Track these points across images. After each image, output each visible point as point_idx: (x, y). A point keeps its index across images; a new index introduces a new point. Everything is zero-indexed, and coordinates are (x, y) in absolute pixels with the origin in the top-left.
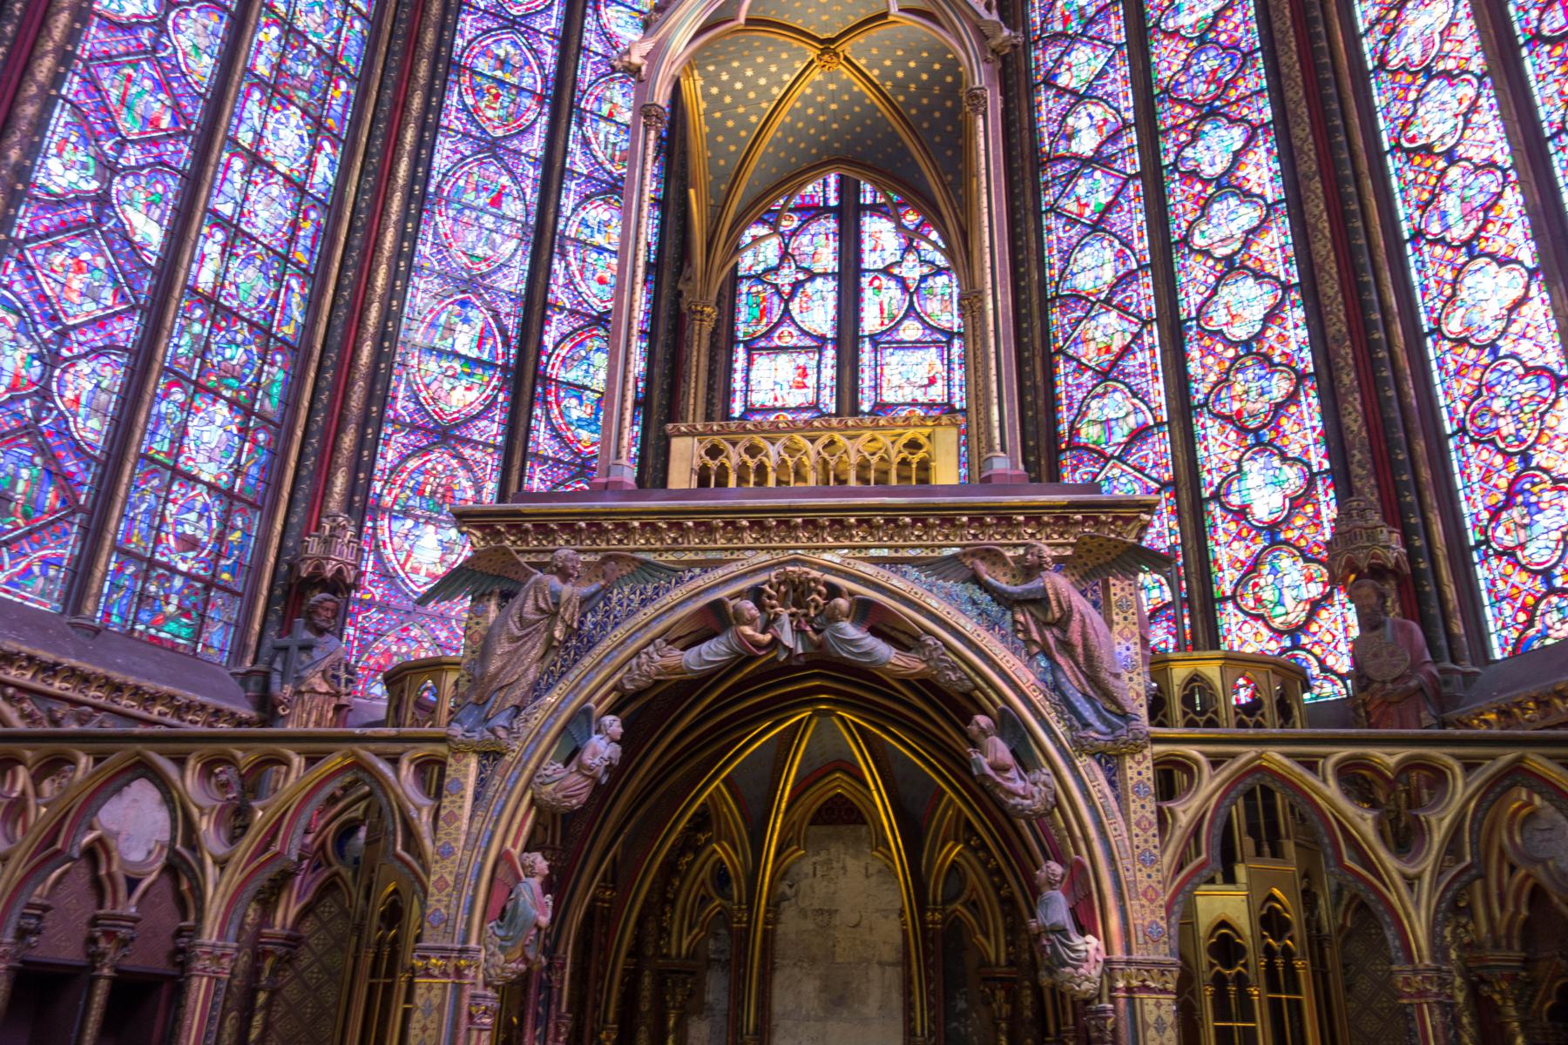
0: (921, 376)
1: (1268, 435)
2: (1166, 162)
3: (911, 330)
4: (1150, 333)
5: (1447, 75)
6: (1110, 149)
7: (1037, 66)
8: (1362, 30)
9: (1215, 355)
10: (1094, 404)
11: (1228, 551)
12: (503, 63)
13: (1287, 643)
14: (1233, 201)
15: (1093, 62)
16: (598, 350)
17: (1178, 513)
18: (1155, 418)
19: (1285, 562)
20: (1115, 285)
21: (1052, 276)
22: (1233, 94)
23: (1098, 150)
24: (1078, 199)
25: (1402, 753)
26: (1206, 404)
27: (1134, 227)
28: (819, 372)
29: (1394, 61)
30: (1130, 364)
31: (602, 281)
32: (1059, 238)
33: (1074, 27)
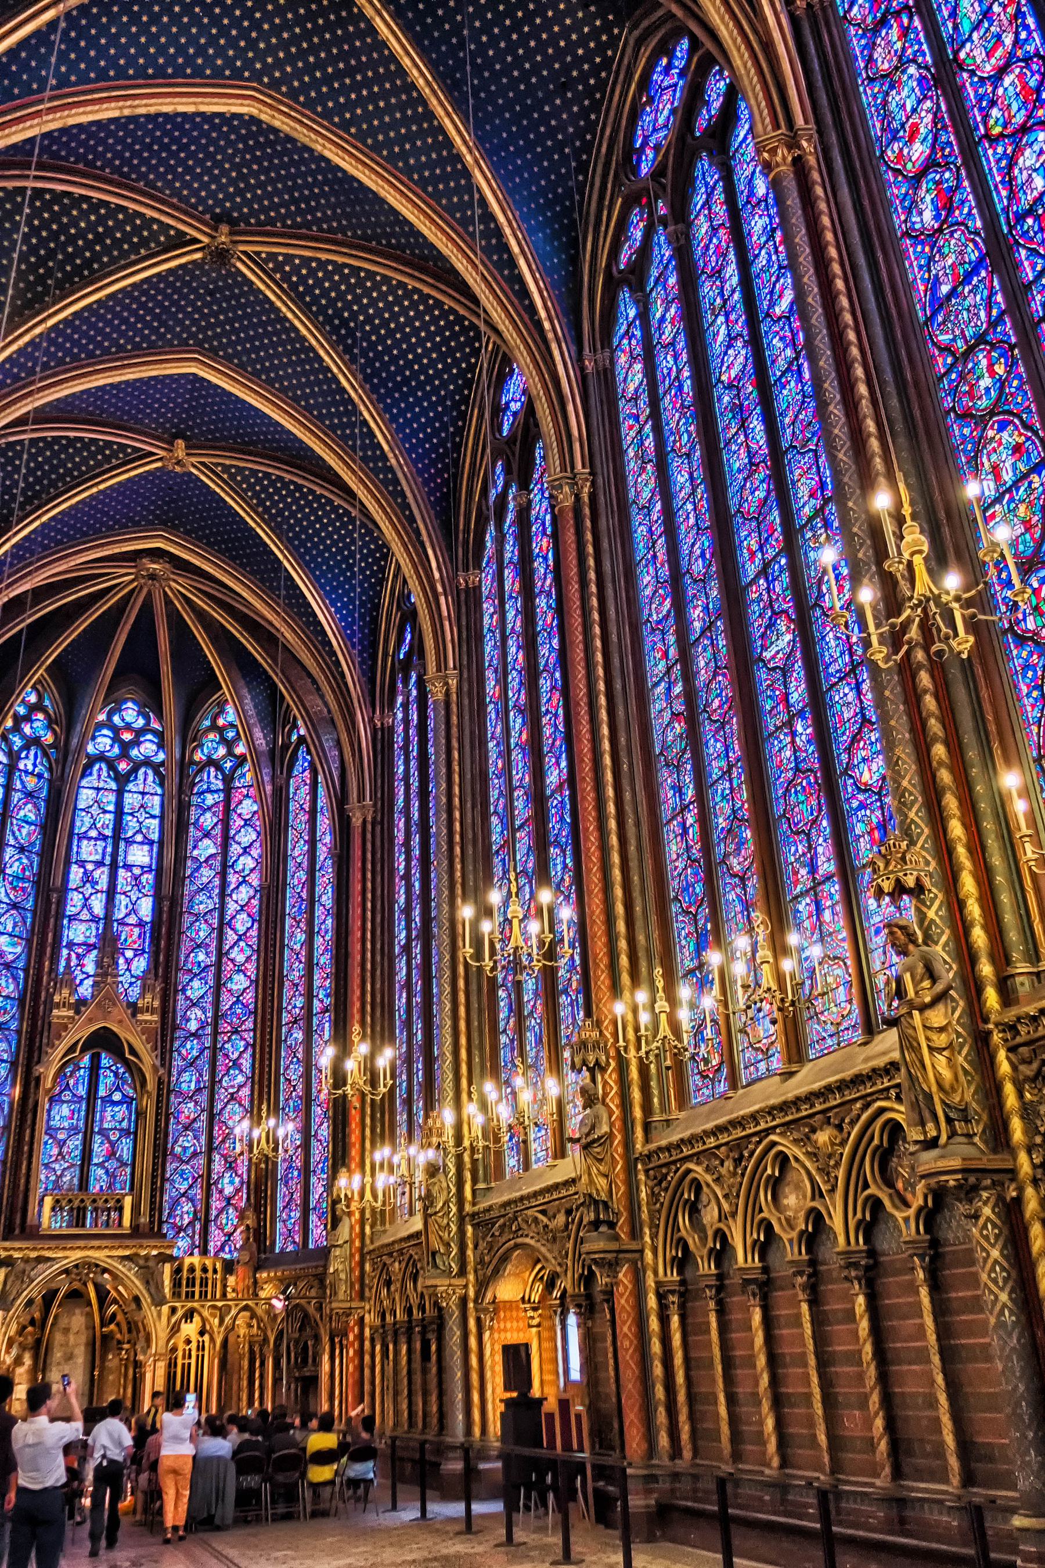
11: (216, 1204)
30: (196, 1125)
33: (196, 970)
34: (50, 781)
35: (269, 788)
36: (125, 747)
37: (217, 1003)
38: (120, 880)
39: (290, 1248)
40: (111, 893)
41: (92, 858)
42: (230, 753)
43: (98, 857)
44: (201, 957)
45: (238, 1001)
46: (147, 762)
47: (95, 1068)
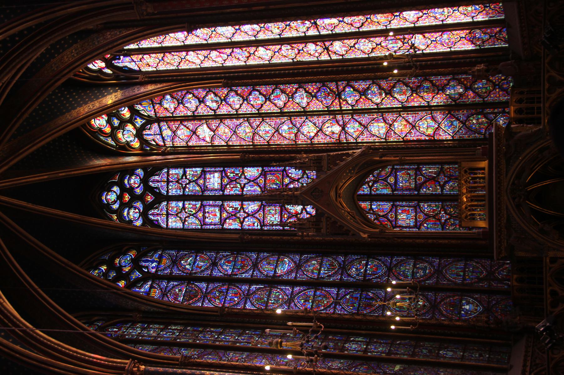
0: (406, 177)
1: (440, 88)
3: (392, 180)
5: (355, 44)
6: (341, 123)
7: (305, 142)
8: (329, 58)
9: (414, 99)
10: (421, 130)
12: (306, 301)
14: (370, 92)
16: (400, 269)
17: (458, 111)
19: (476, 86)
20: (386, 123)
23: (340, 126)
24: (355, 132)
25: (546, 83)
28: (404, 206)
29: (344, 53)
30: (411, 120)
31: (377, 269)
33: (295, 131)
34: (164, 250)
35: (150, 88)
36: (135, 198)
37: (318, 113)
38: (232, 192)
39: (504, 34)
40: (241, 198)
41: (218, 215)
42: (131, 121)
43: (217, 210)
44: (285, 127)
45: (315, 96)
46: (145, 181)
47: (371, 198)
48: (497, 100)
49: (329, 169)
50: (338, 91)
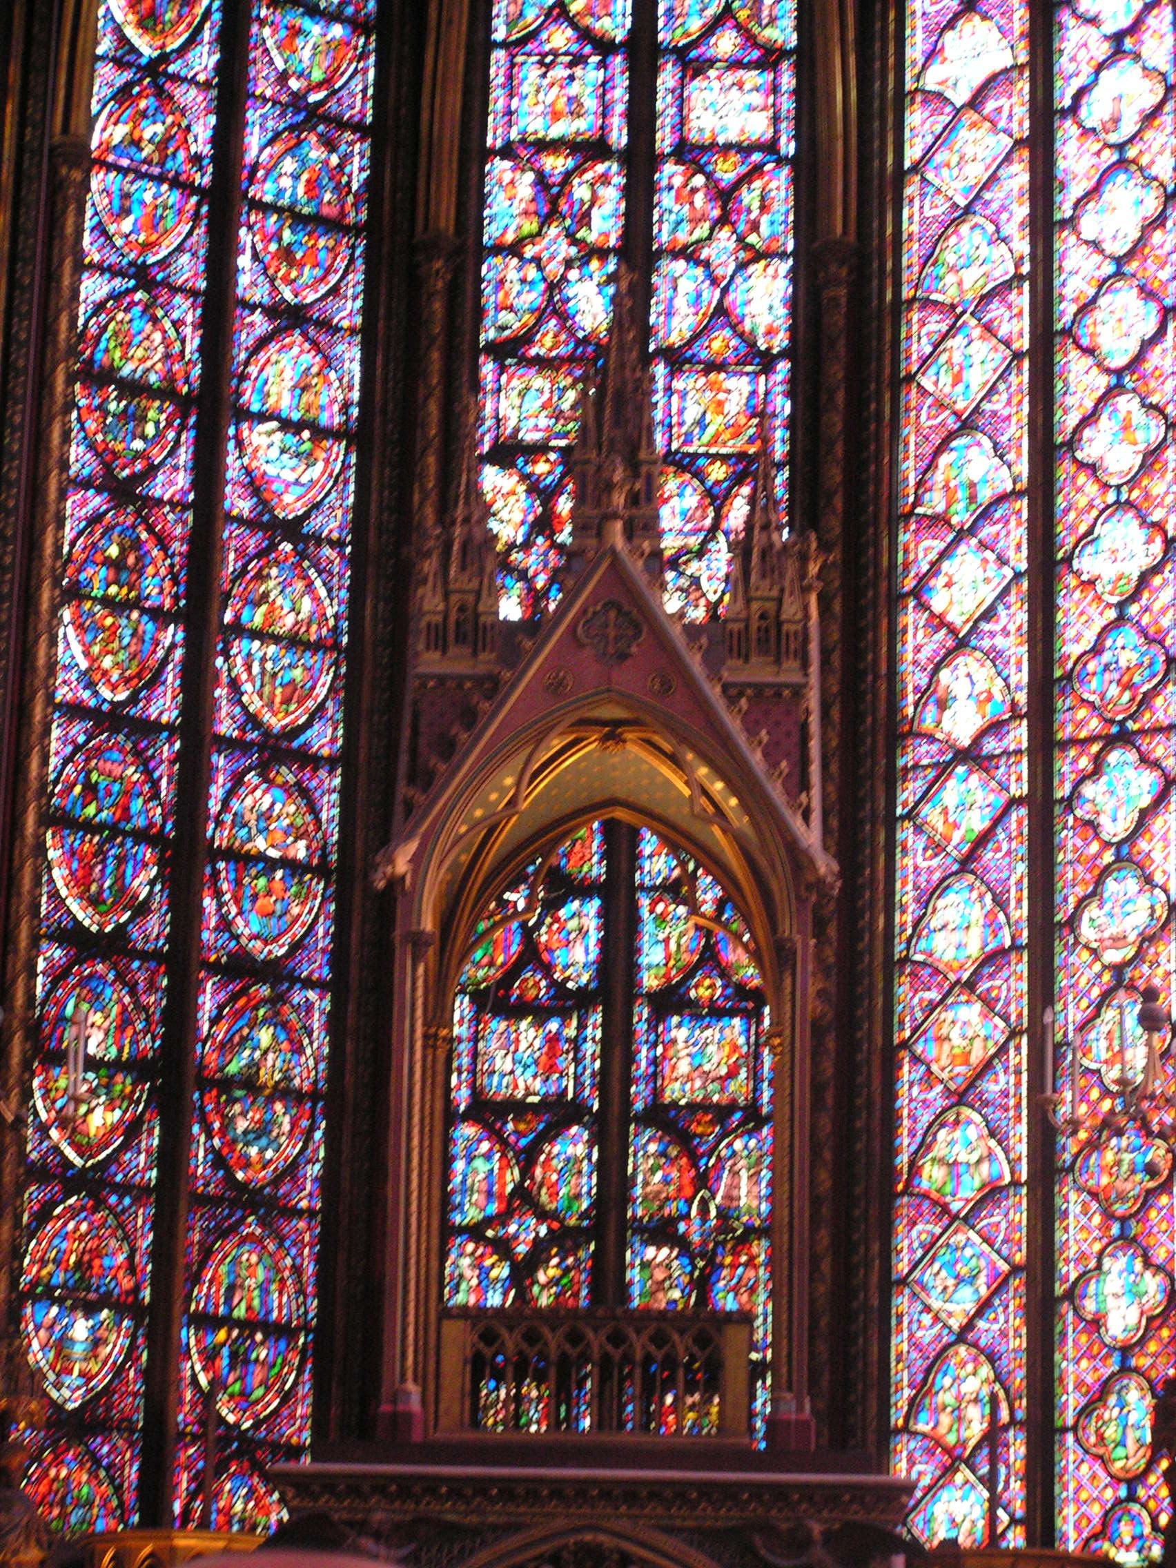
0: (716, 1059)
1: (1135, 1228)
2: (1059, 794)
4: (1018, 1048)
6: (991, 745)
11: (1076, 1370)
13: (1123, 1492)
14: (1132, 885)
15: (981, 586)
18: (1012, 1173)
19: (1133, 1396)
20: (983, 964)
21: (903, 925)
22: (1147, 719)
23: (978, 739)
24: (945, 811)
26: (1071, 1169)
27: (1013, 880)
30: (991, 1087)
32: (916, 867)
33: (961, 515)
45: (1121, 620)
48: (1065, 1492)
49: (732, 693)
50: (1141, 732)
